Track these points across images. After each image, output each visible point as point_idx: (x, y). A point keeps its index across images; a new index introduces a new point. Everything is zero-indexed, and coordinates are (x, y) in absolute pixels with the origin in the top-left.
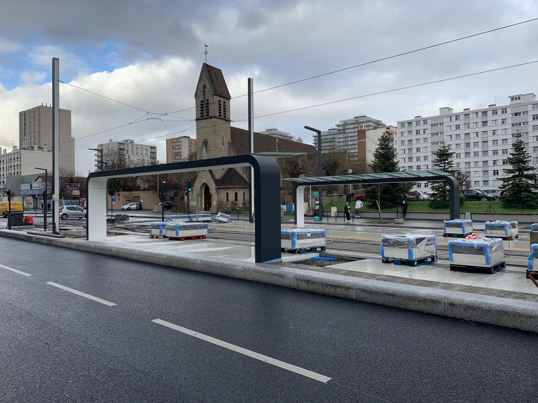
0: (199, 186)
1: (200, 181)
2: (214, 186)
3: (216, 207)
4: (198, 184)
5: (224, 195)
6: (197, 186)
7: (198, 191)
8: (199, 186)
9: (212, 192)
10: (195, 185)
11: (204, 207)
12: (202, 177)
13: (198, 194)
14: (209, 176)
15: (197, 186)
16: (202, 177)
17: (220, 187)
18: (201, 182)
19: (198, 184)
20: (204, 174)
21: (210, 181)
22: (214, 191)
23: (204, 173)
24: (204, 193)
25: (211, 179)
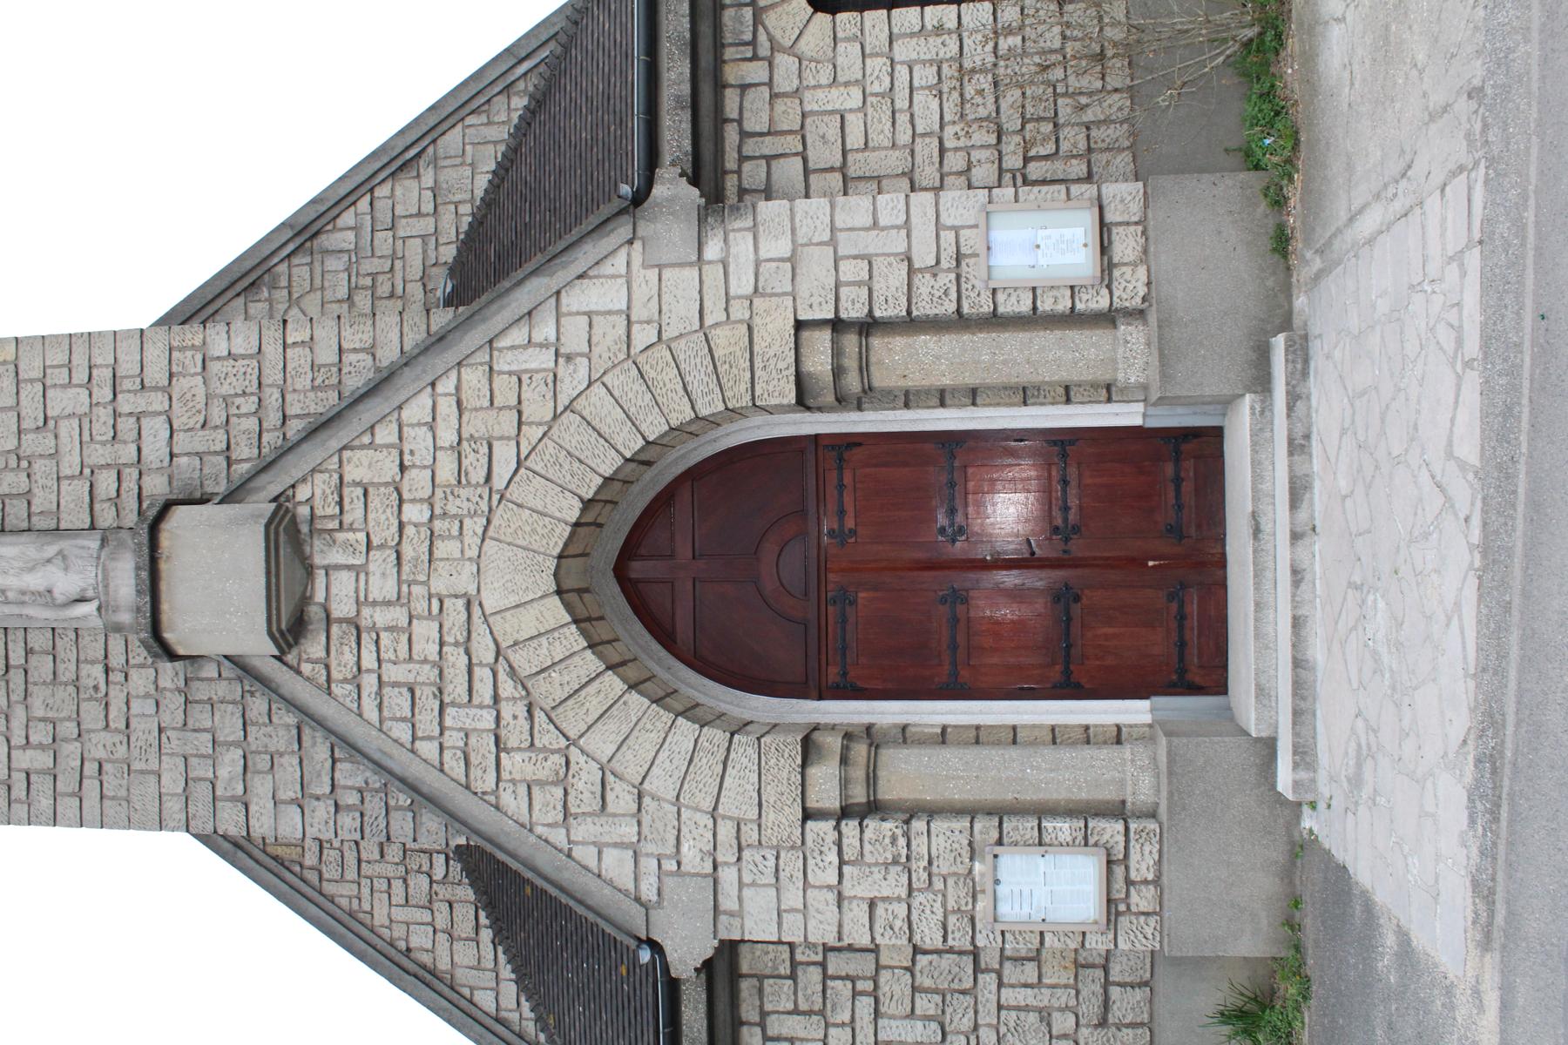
0: (631, 765)
1: (515, 734)
2: (645, 280)
3: (1123, 196)
4: (586, 778)
5: (849, 55)
6: (622, 799)
7: (739, 800)
8: (631, 765)
9: (775, 329)
10: (617, 866)
11: (1135, 712)
12: (425, 631)
13: (825, 792)
14: (419, 441)
15: (622, 799)
16: (425, 631)
17: (675, 135)
18: (549, 690)
19: (586, 778)
20: (382, 585)
21: (538, 408)
22: (742, 283)
23: (340, 594)
24: (820, 698)
25: (473, 378)
